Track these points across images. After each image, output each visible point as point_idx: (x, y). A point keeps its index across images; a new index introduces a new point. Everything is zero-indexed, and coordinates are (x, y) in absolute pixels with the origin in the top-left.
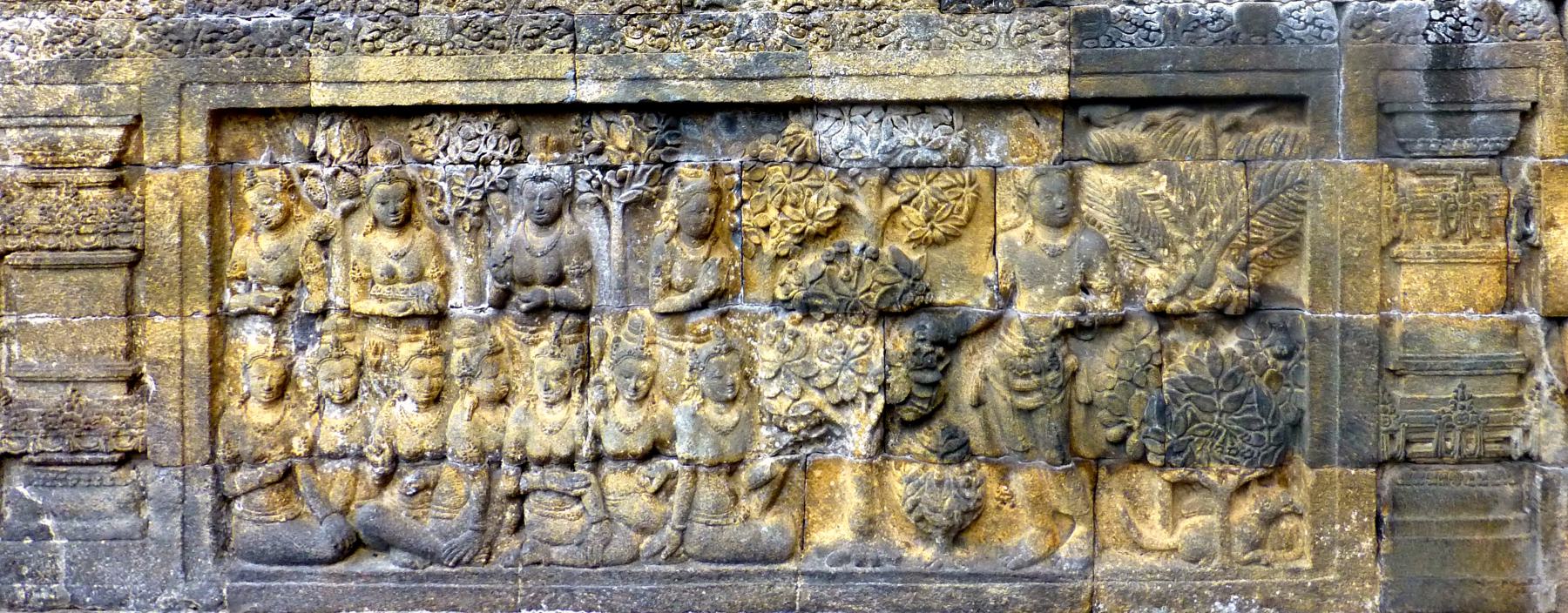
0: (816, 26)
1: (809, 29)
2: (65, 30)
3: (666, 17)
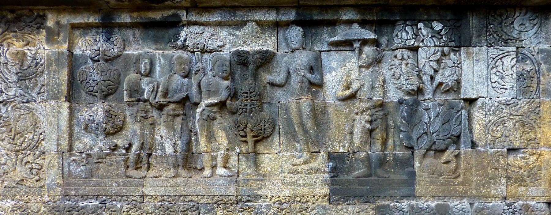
0: (285, 209)
1: (283, 210)
2: (17, 207)
3: (232, 205)
